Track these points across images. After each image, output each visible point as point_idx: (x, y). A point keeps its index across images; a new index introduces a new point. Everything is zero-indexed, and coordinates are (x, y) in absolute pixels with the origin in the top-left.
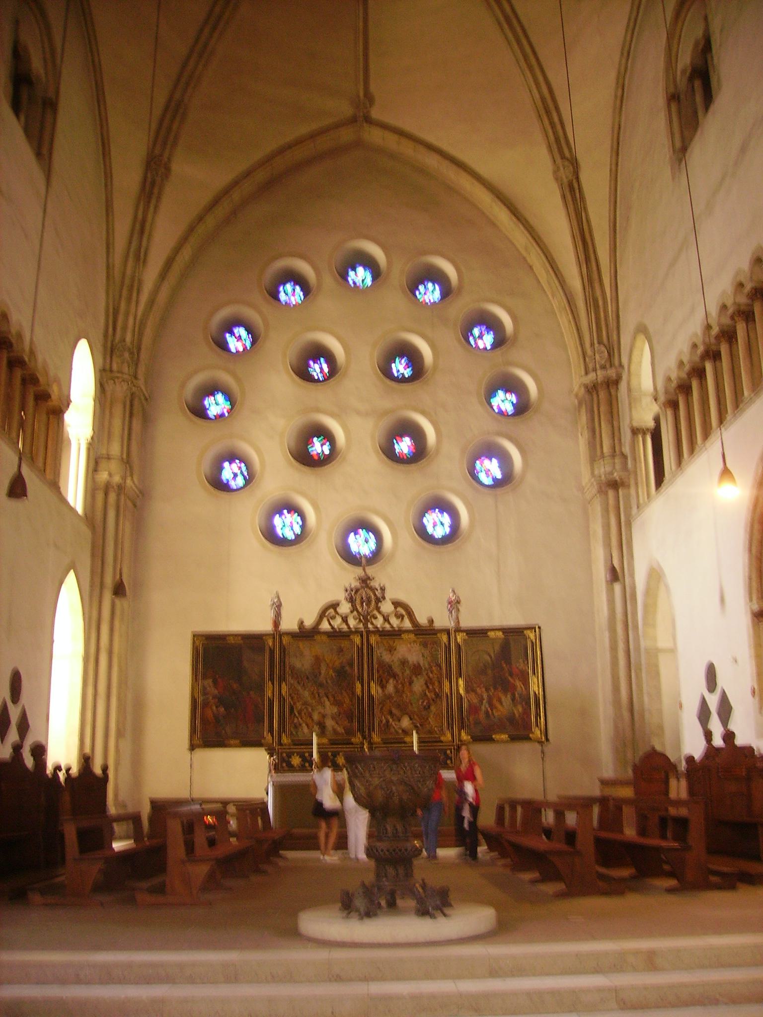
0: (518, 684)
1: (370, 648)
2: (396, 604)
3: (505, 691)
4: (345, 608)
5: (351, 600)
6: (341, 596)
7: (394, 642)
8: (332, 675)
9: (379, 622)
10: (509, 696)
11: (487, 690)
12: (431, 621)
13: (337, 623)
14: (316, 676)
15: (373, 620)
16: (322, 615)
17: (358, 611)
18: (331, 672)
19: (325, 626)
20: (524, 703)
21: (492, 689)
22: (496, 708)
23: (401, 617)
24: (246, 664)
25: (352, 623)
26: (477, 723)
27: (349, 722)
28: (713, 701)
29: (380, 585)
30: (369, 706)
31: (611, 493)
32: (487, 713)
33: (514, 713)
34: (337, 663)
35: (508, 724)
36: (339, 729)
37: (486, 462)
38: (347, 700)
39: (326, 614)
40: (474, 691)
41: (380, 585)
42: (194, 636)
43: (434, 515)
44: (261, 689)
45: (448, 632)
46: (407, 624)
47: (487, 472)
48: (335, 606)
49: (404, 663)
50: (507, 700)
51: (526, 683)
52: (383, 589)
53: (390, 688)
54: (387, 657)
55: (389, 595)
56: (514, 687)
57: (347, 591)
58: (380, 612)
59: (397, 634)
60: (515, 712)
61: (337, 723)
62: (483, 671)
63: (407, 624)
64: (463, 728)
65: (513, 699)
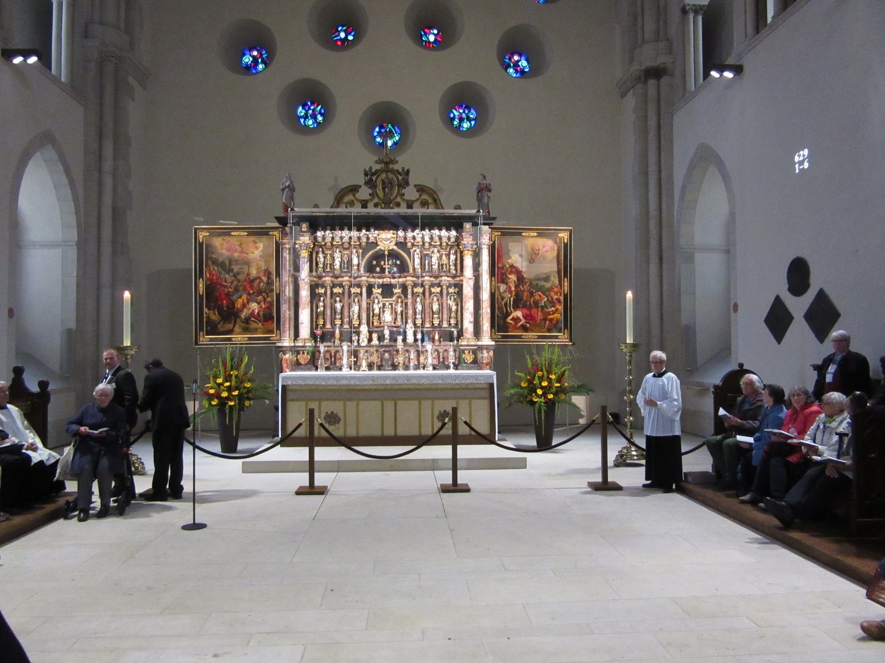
2: (421, 189)
5: (370, 183)
6: (361, 180)
28: (798, 306)
29: (403, 169)
30: (195, 267)
31: (652, 82)
37: (516, 58)
41: (403, 169)
43: (461, 111)
47: (516, 65)
48: (354, 189)
52: (407, 173)
55: (413, 180)
57: (366, 174)
58: (403, 200)
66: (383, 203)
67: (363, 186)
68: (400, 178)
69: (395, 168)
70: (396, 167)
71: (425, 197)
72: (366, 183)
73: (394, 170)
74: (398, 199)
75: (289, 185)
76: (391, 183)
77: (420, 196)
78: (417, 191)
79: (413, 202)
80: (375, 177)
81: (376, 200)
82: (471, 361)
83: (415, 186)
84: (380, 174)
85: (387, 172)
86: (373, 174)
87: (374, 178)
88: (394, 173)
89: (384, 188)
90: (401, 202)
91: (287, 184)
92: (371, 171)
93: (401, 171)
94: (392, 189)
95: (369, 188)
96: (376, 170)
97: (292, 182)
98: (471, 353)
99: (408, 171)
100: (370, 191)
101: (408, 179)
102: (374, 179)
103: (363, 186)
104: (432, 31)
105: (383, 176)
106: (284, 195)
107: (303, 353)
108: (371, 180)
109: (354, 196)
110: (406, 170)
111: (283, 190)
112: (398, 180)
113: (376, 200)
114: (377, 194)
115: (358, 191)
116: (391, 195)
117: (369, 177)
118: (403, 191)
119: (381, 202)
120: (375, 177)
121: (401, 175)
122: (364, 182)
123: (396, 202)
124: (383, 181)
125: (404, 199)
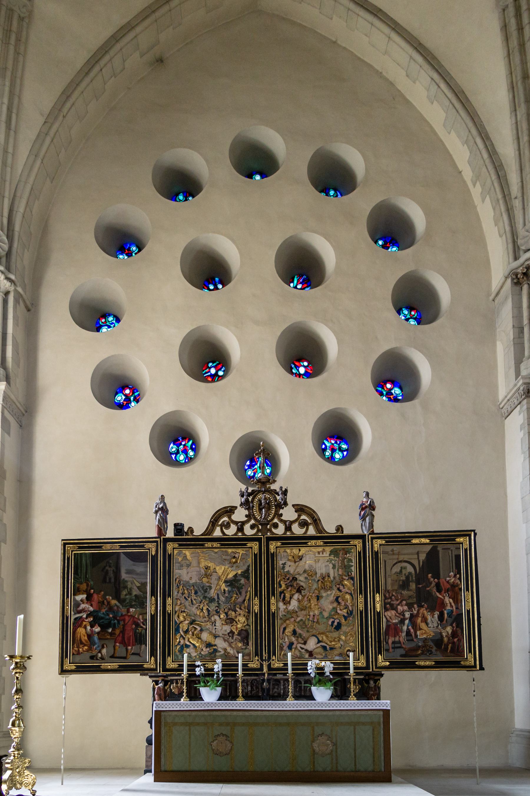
0: (447, 600)
1: (272, 557)
2: (300, 509)
3: (432, 610)
4: (240, 515)
5: (246, 504)
6: (237, 501)
7: (300, 550)
8: (224, 590)
9: (280, 530)
10: (436, 616)
11: (410, 606)
12: (339, 528)
13: (232, 531)
14: (205, 591)
15: (273, 530)
16: (214, 522)
17: (255, 519)
18: (223, 586)
19: (217, 533)
20: (454, 625)
21: (415, 606)
22: (420, 629)
23: (304, 524)
24: (124, 576)
25: (248, 531)
26: (397, 645)
27: (244, 645)
29: (281, 488)
32: (408, 633)
33: (442, 636)
34: (231, 576)
35: (435, 648)
36: (232, 652)
38: (242, 619)
39: (220, 523)
40: (393, 608)
41: (281, 488)
42: (65, 545)
44: (141, 603)
45: (362, 537)
46: (312, 531)
48: (230, 511)
49: (310, 573)
50: (433, 619)
51: (457, 600)
52: (285, 493)
53: (294, 604)
54: (290, 568)
55: (291, 499)
56: (443, 605)
57: (242, 496)
58: (282, 521)
59: (302, 541)
60: (444, 634)
61: (230, 646)
62: (405, 585)
63: (312, 531)
64: (380, 653)
65: (441, 618)
66: (261, 524)
67: (239, 508)
68: (278, 498)
69: (272, 488)
70: (273, 487)
71: (303, 517)
72: (242, 505)
73: (272, 490)
74: (276, 520)
75: (162, 507)
76: (268, 504)
77: (299, 516)
78: (296, 511)
79: (292, 522)
80: (251, 497)
81: (253, 522)
82: (357, 691)
83: (293, 506)
84: (257, 494)
85: (264, 492)
86: (249, 495)
87: (250, 499)
88: (271, 493)
89: (260, 510)
90: (280, 524)
91: (161, 506)
92: (247, 491)
93: (278, 490)
94: (269, 509)
95: (245, 509)
96: (252, 491)
97: (165, 504)
98: (357, 682)
99: (286, 491)
100: (247, 512)
101: (286, 499)
102: (250, 499)
103: (239, 508)
104: (302, 364)
105: (261, 496)
106: (158, 517)
107: (177, 683)
108: (247, 501)
109: (230, 517)
110: (283, 489)
111: (156, 512)
112: (276, 500)
113: (253, 522)
114: (254, 515)
115: (234, 513)
116: (269, 516)
117: (245, 497)
118: (281, 511)
119: (257, 523)
120: (251, 497)
121: (279, 495)
122: (240, 503)
123: (274, 523)
124: (260, 501)
125: (282, 519)
